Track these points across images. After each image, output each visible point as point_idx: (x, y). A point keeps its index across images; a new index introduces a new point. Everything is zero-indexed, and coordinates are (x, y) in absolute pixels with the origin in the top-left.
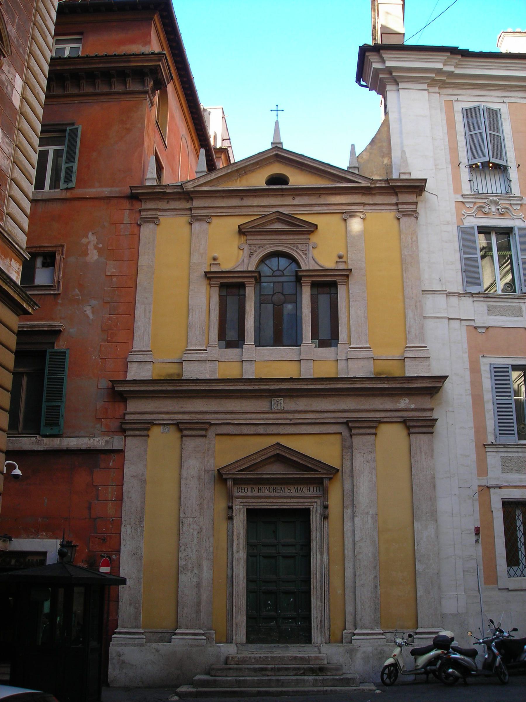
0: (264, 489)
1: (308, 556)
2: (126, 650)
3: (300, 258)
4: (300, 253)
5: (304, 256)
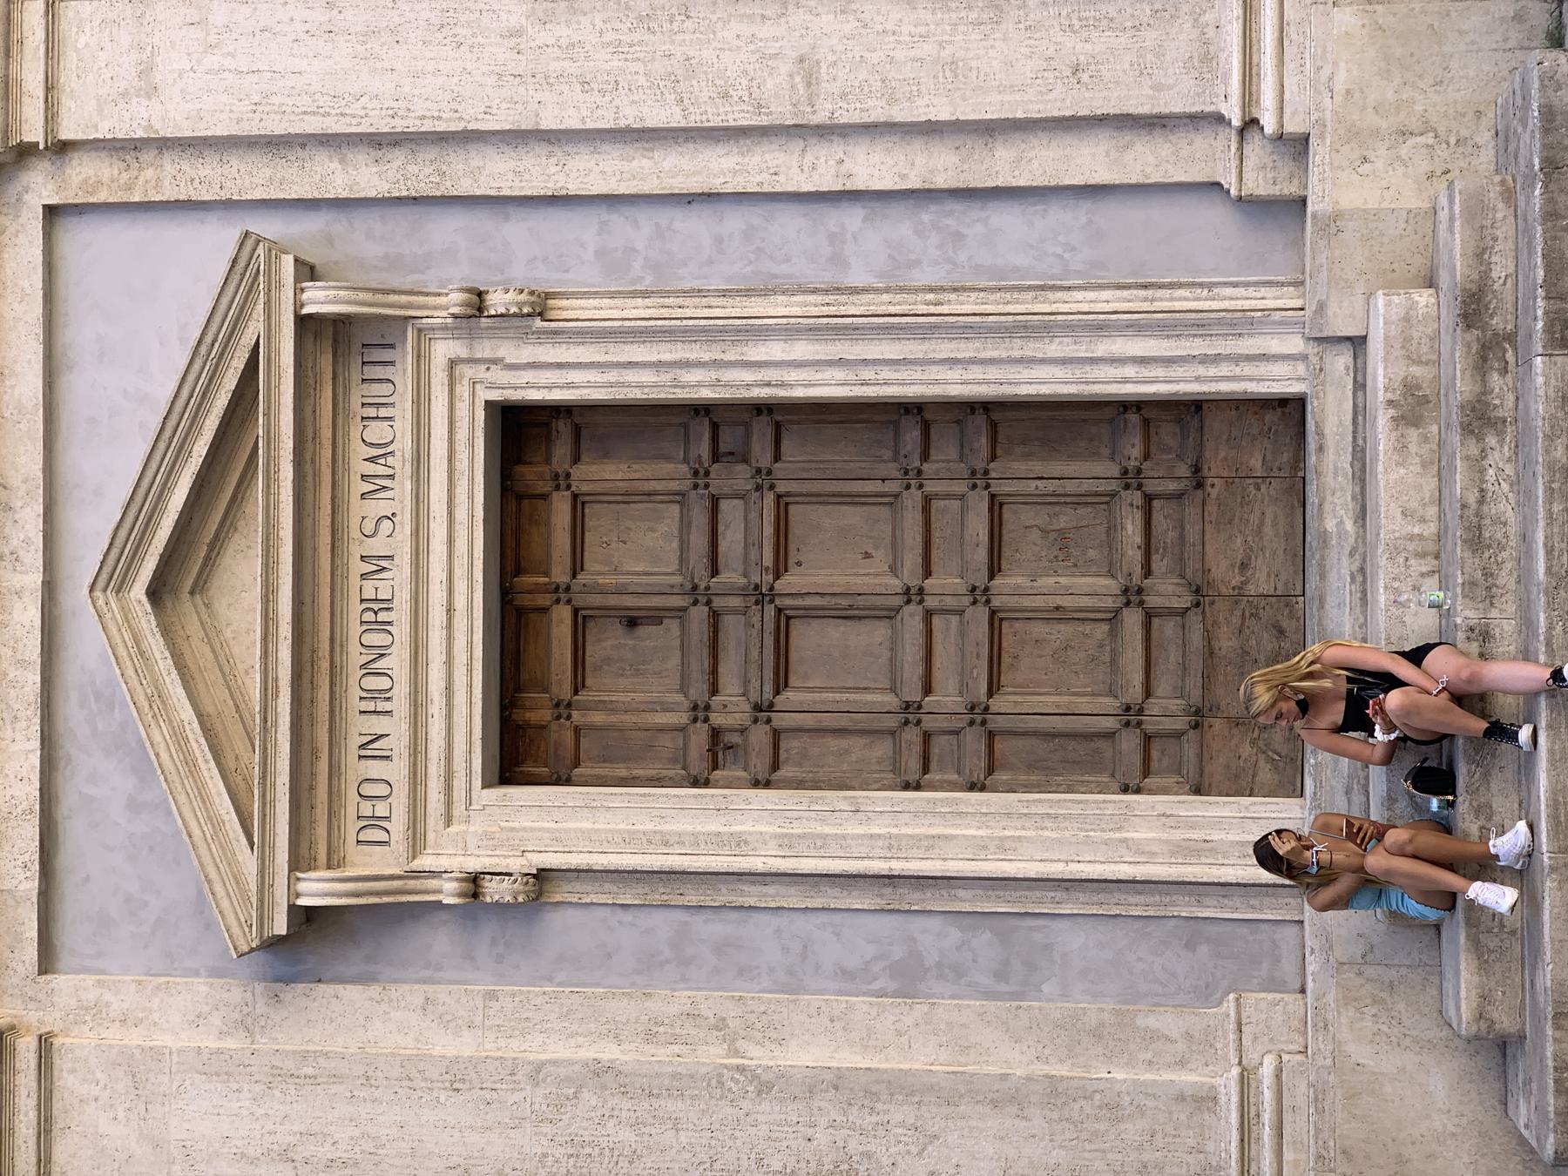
1: (779, 418)
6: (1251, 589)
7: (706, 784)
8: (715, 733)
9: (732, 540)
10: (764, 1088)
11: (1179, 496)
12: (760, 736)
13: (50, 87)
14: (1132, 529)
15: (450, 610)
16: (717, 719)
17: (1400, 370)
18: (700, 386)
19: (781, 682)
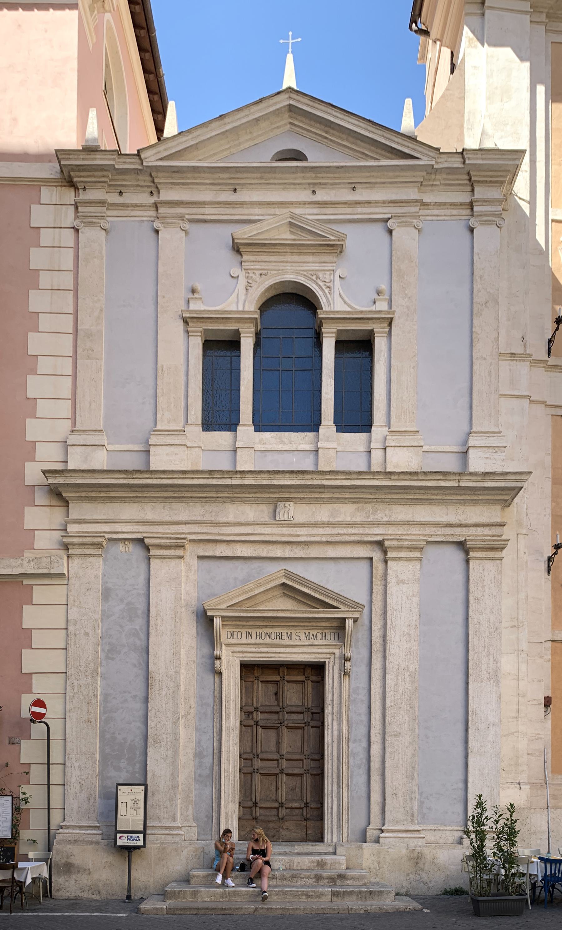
0: (263, 635)
2: (75, 850)
3: (321, 293)
4: (321, 284)
5: (327, 291)
6: (282, 830)
7: (241, 711)
8: (252, 713)
9: (294, 717)
10: (175, 723)
11: (303, 815)
12: (251, 722)
13: (400, 558)
14: (296, 805)
15: (279, 653)
16: (255, 713)
17: (329, 862)
18: (328, 710)
19: (263, 727)
